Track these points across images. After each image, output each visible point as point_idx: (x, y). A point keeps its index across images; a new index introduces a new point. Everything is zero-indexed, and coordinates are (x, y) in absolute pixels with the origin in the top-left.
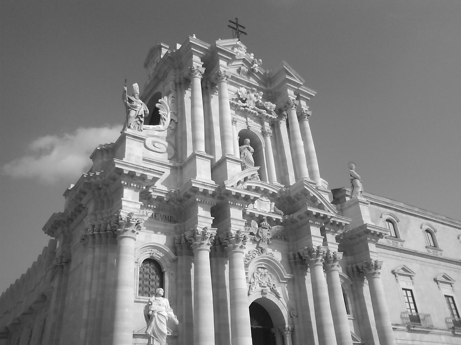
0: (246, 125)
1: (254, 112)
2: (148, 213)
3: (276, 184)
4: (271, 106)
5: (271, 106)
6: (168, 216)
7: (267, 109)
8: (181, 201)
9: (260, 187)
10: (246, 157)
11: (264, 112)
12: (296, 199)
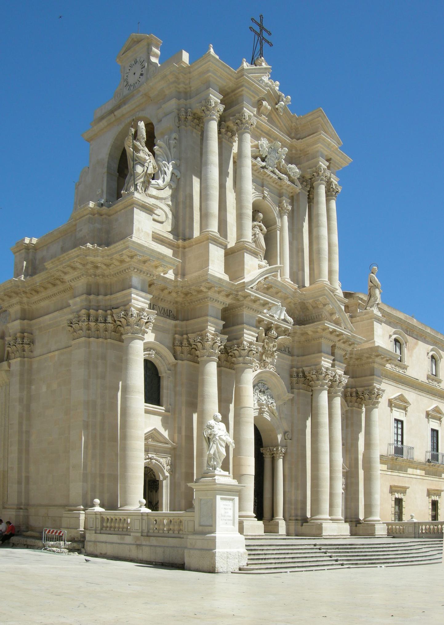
1: (274, 176)
4: (294, 170)
8: (186, 294)
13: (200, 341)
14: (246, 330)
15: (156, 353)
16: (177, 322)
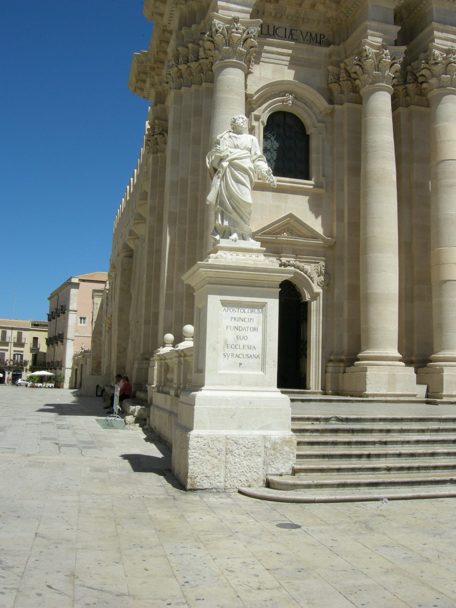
2: (277, 29)
6: (316, 35)
13: (358, 62)
14: (438, 31)
15: (295, 98)
16: (332, 47)
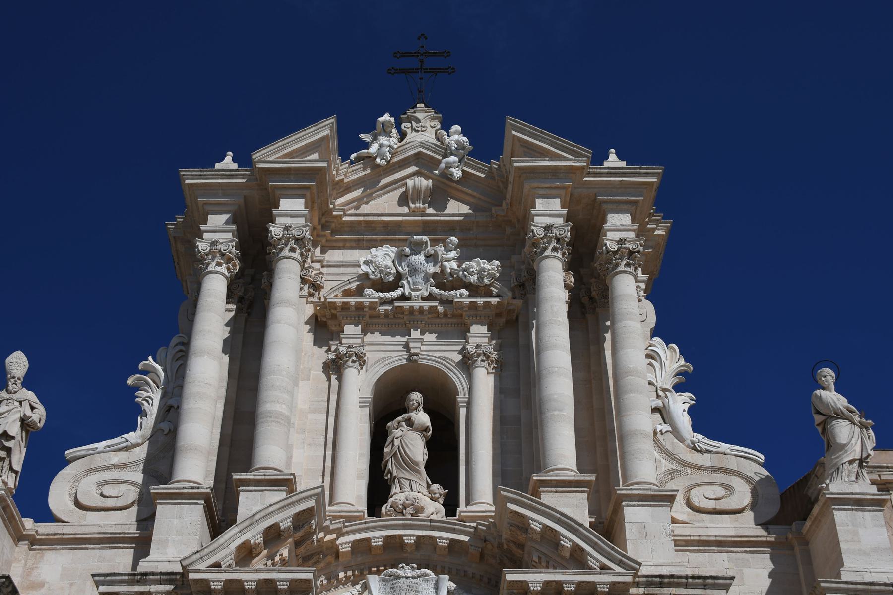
0: (405, 353)
1: (426, 305)
3: (486, 511)
5: (480, 272)
7: (471, 283)
9: (401, 537)
10: (399, 448)
11: (461, 296)
12: (514, 549)
